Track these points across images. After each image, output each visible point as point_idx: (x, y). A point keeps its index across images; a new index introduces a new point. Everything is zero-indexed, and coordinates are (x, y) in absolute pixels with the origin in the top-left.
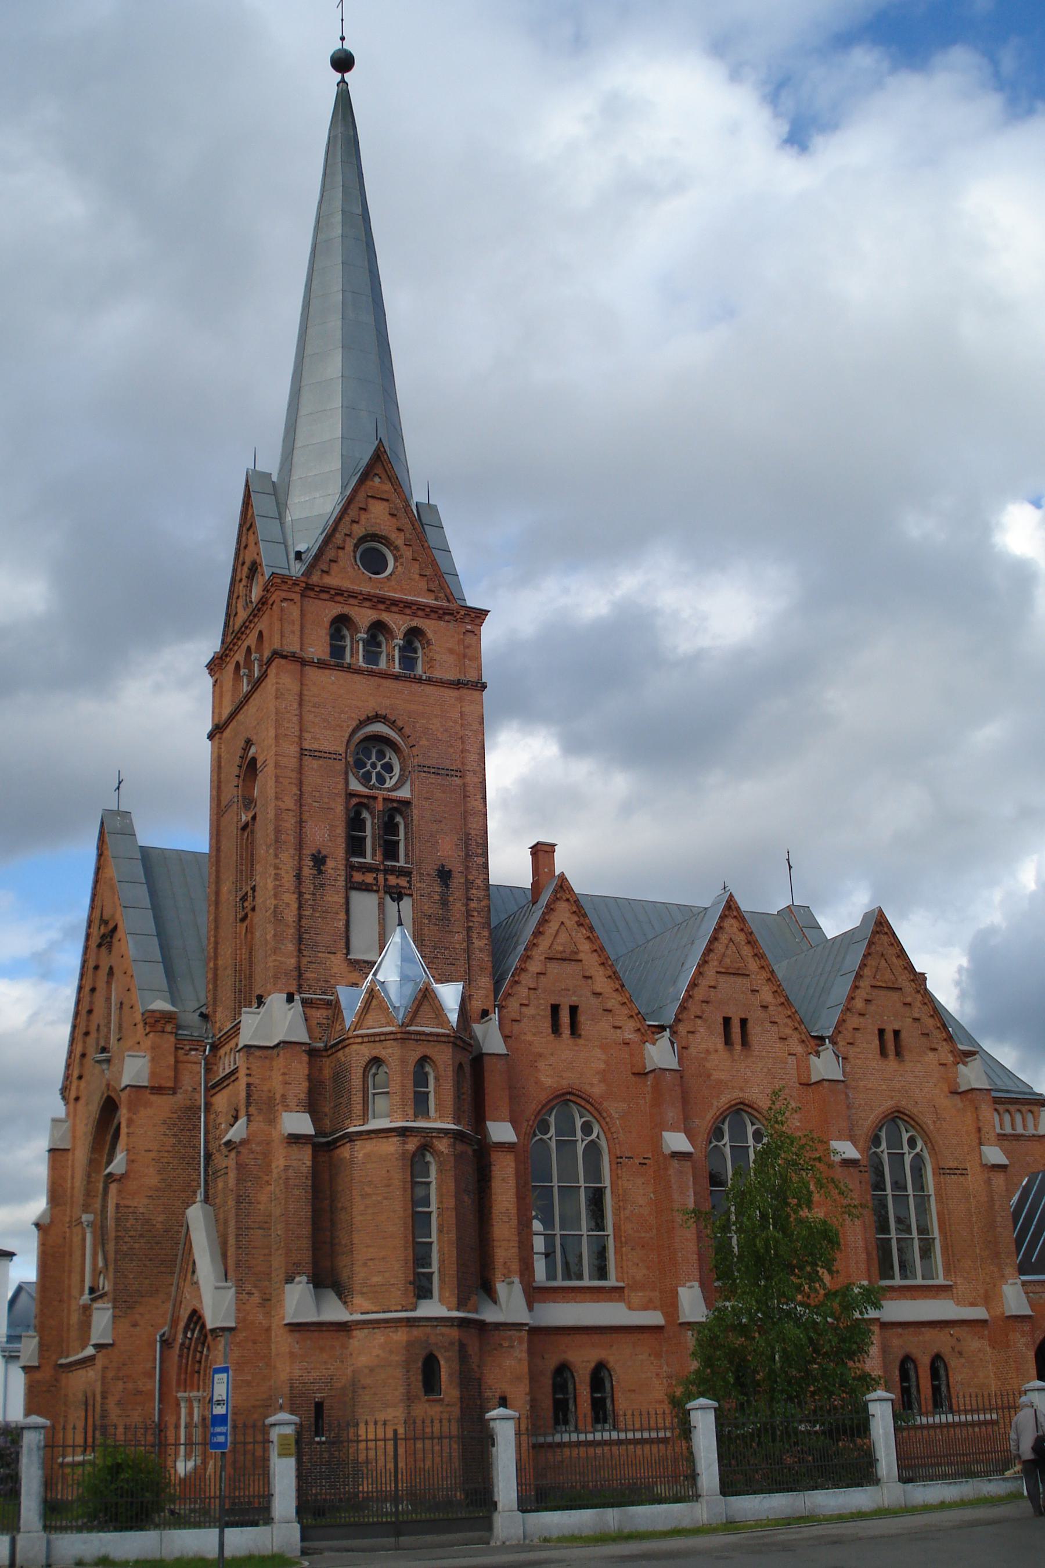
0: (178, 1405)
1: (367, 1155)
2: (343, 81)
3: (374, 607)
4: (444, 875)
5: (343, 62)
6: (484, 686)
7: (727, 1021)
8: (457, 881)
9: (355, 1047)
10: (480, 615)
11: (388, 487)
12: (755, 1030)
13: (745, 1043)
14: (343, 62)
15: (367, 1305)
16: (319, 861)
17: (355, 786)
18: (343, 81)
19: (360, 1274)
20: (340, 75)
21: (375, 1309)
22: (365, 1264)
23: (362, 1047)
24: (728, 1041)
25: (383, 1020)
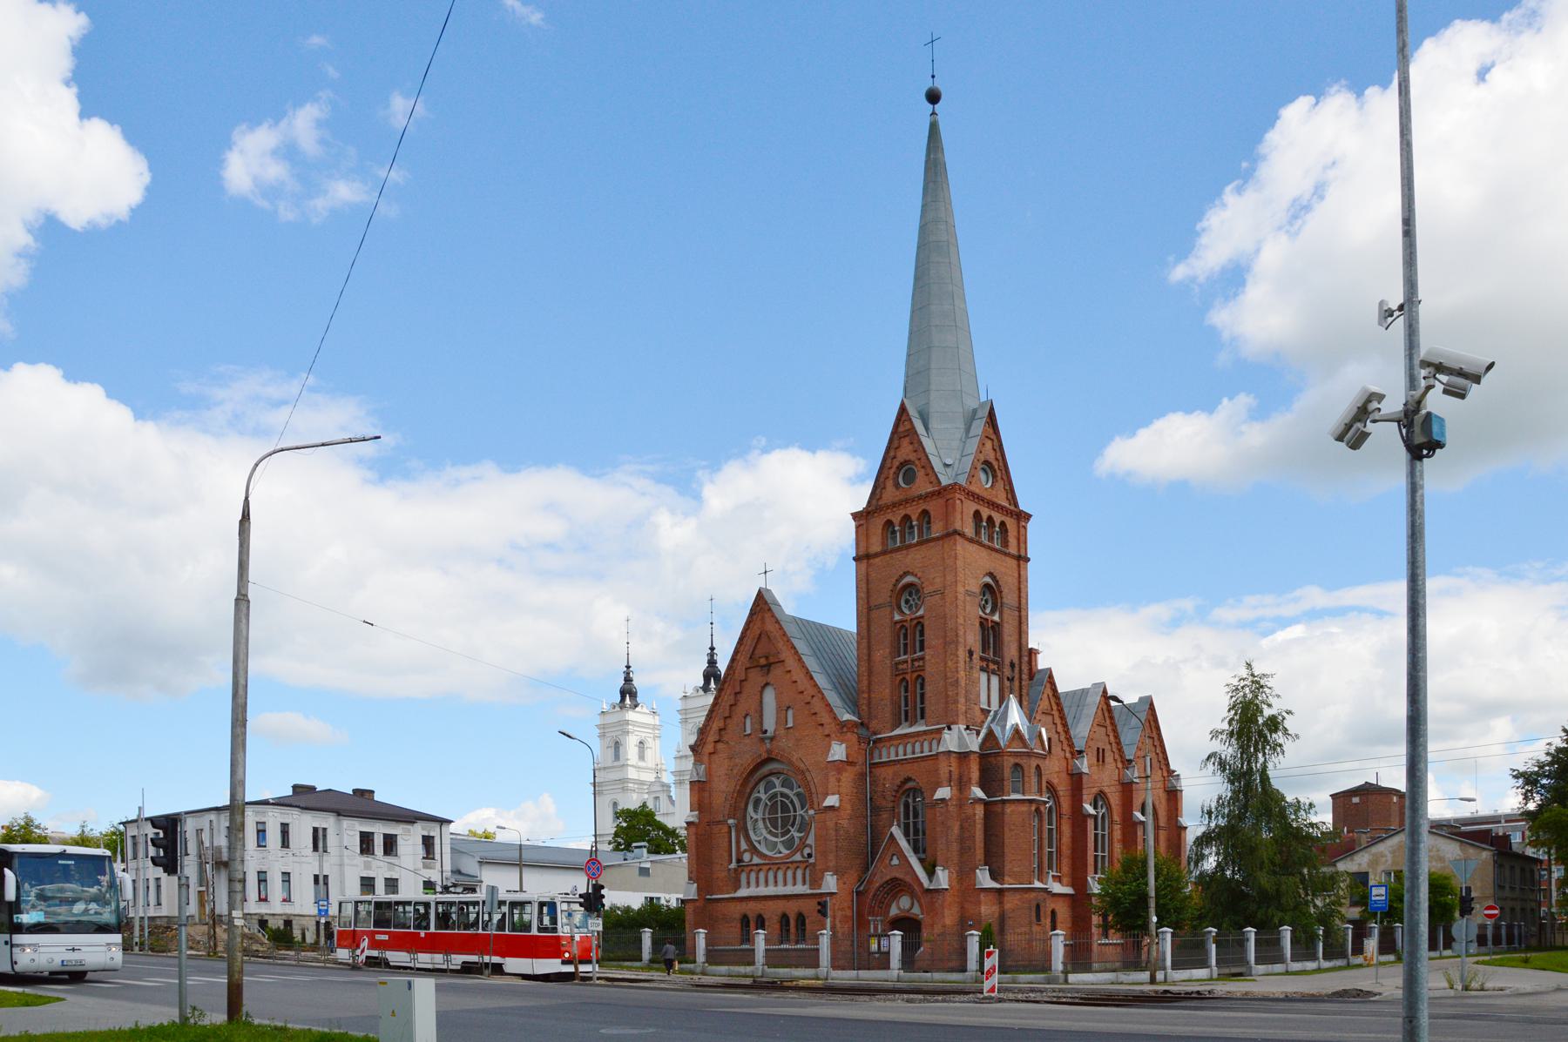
0: (869, 924)
1: (1012, 811)
2: (933, 113)
3: (988, 507)
4: (1012, 665)
5: (933, 97)
6: (1028, 560)
7: (1098, 749)
8: (1017, 669)
9: (1006, 757)
10: (1028, 517)
11: (991, 431)
12: (1106, 755)
13: (1103, 761)
14: (933, 97)
15: (1011, 881)
16: (971, 653)
17: (981, 613)
18: (933, 113)
19: (1008, 867)
20: (932, 106)
21: (1014, 882)
22: (1010, 862)
23: (1009, 758)
24: (1098, 760)
25: (1021, 745)
